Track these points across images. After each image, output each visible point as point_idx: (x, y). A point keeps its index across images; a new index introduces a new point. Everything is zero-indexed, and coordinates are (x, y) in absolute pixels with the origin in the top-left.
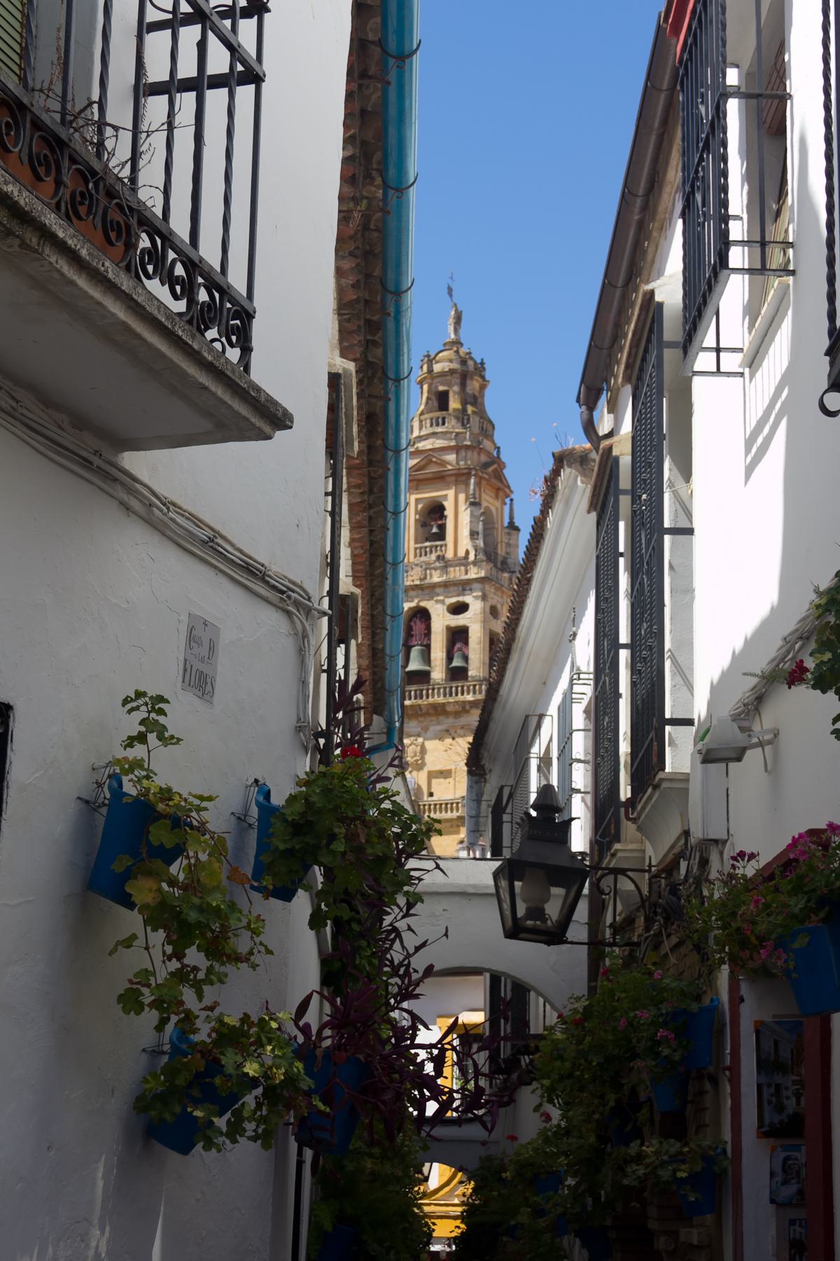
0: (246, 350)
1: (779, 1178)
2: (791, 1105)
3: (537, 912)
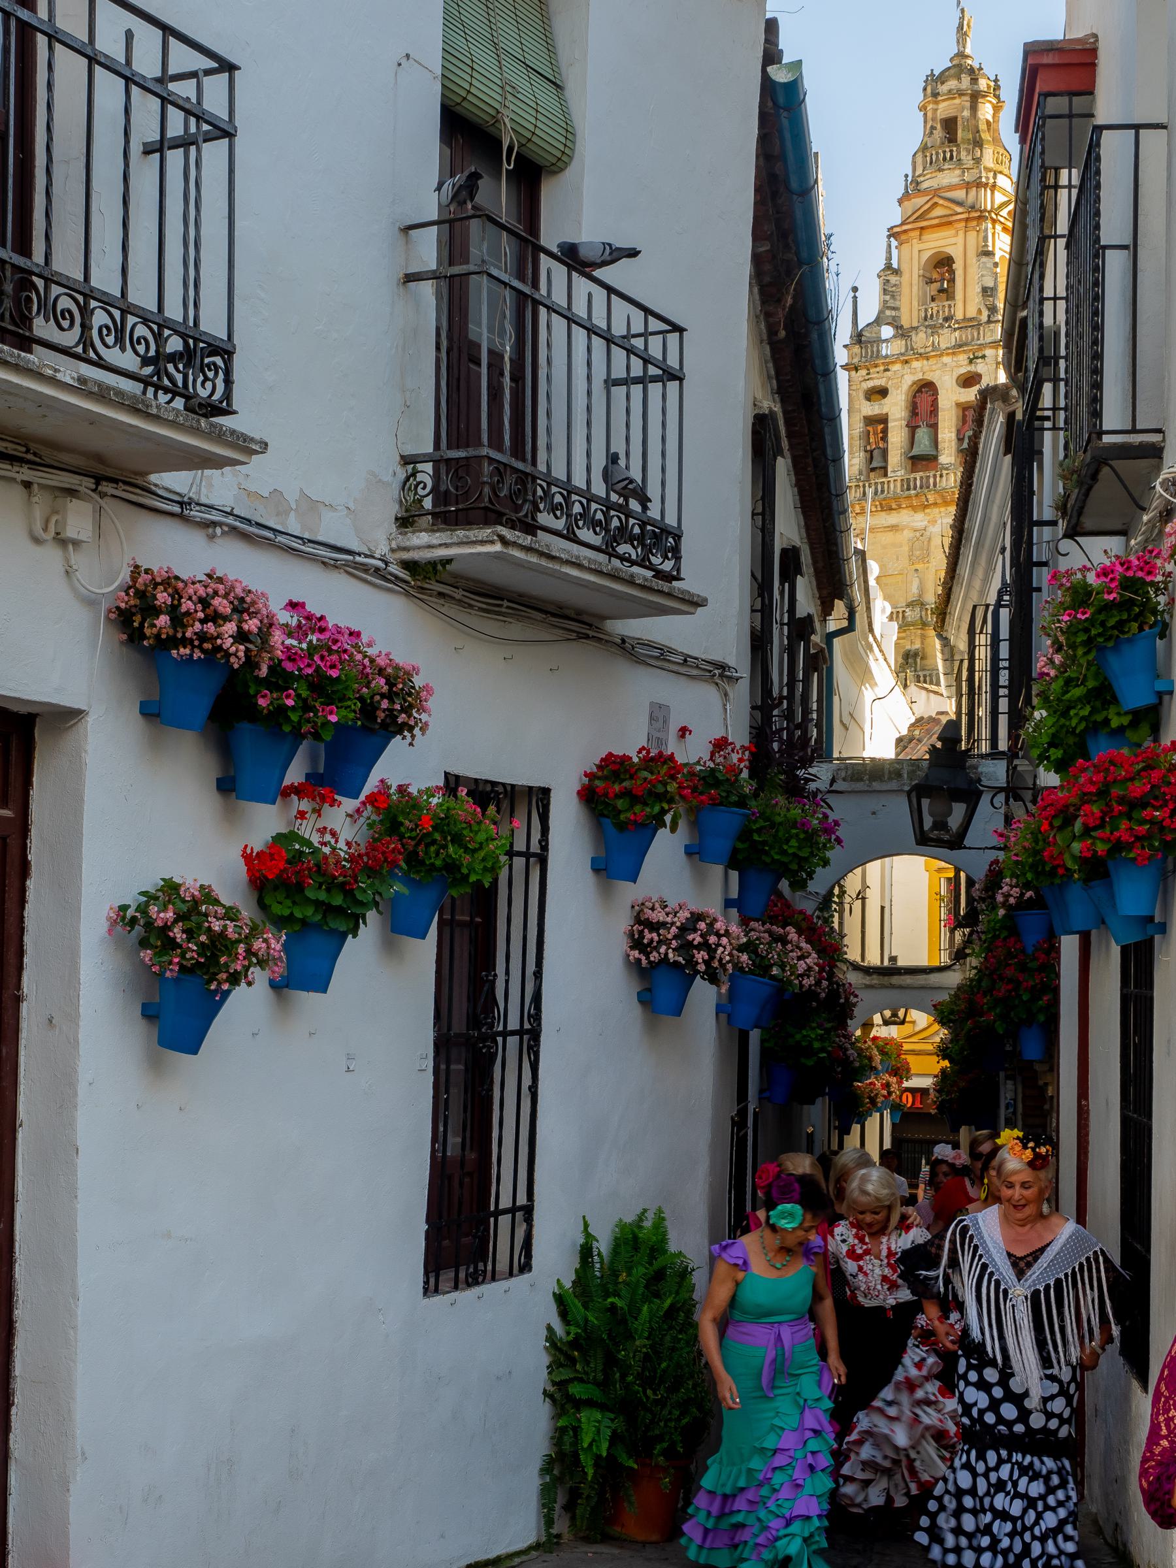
0: (678, 558)
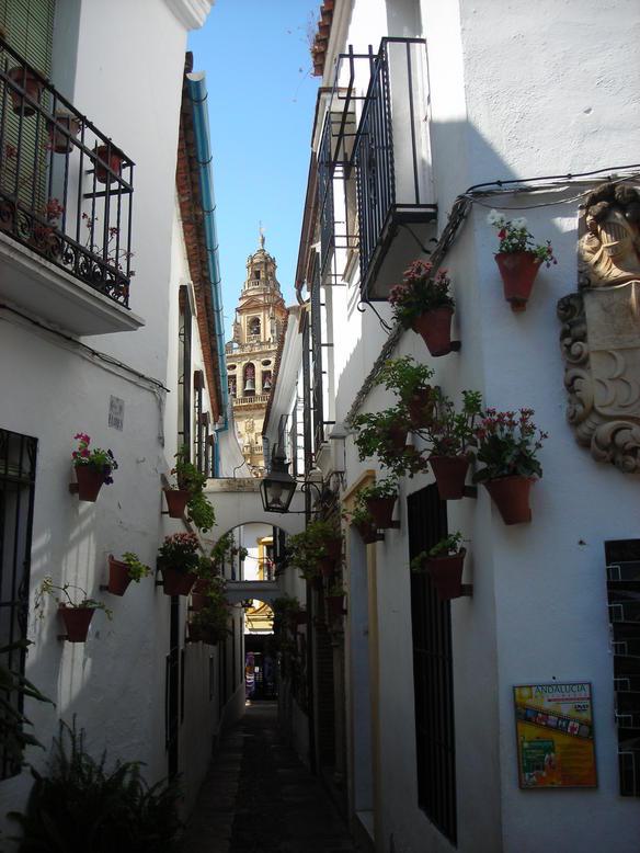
0: (127, 297)
3: (276, 500)
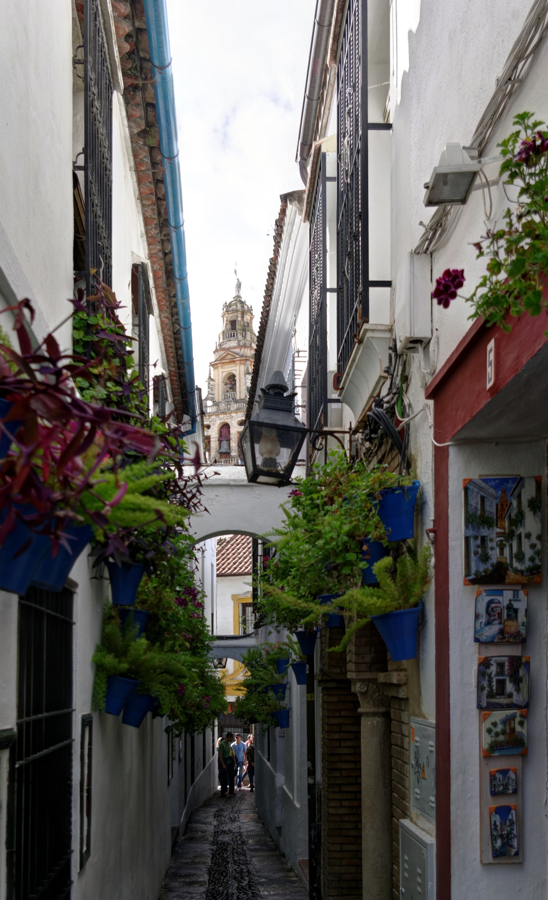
1: (483, 620)
2: (495, 555)
3: (271, 462)
